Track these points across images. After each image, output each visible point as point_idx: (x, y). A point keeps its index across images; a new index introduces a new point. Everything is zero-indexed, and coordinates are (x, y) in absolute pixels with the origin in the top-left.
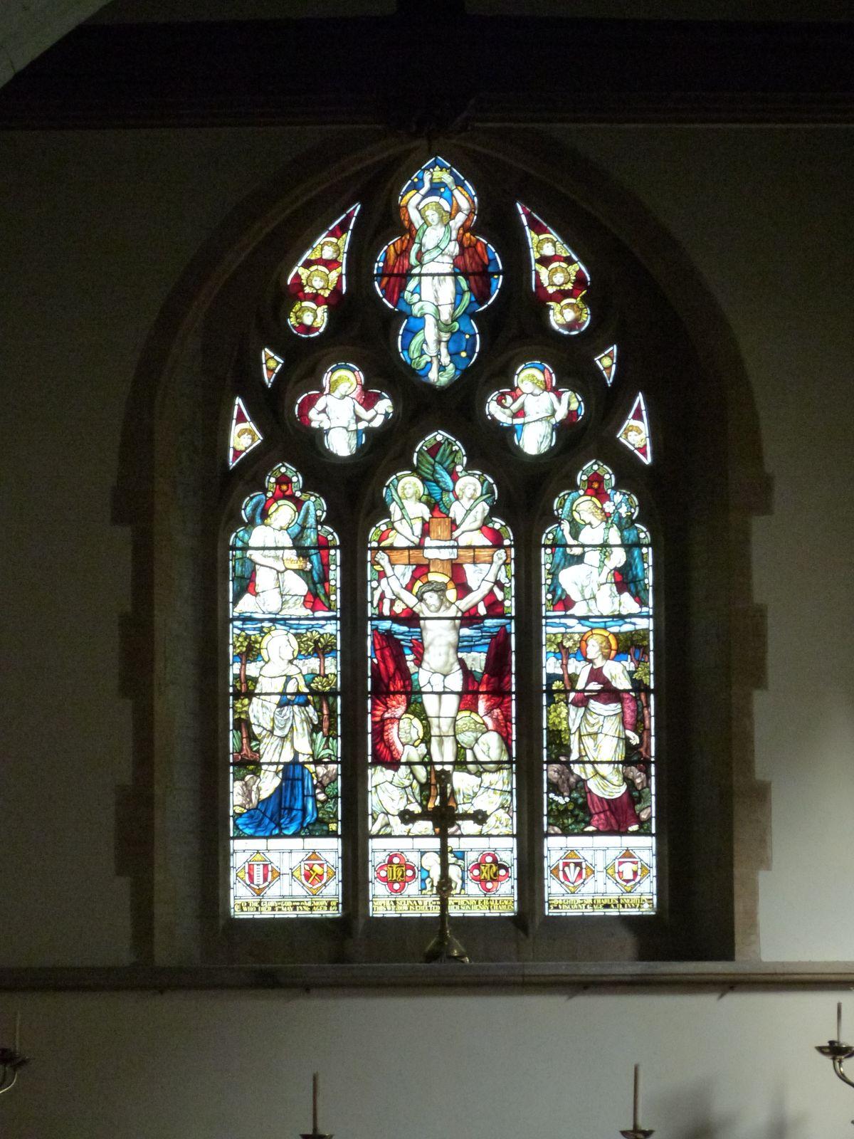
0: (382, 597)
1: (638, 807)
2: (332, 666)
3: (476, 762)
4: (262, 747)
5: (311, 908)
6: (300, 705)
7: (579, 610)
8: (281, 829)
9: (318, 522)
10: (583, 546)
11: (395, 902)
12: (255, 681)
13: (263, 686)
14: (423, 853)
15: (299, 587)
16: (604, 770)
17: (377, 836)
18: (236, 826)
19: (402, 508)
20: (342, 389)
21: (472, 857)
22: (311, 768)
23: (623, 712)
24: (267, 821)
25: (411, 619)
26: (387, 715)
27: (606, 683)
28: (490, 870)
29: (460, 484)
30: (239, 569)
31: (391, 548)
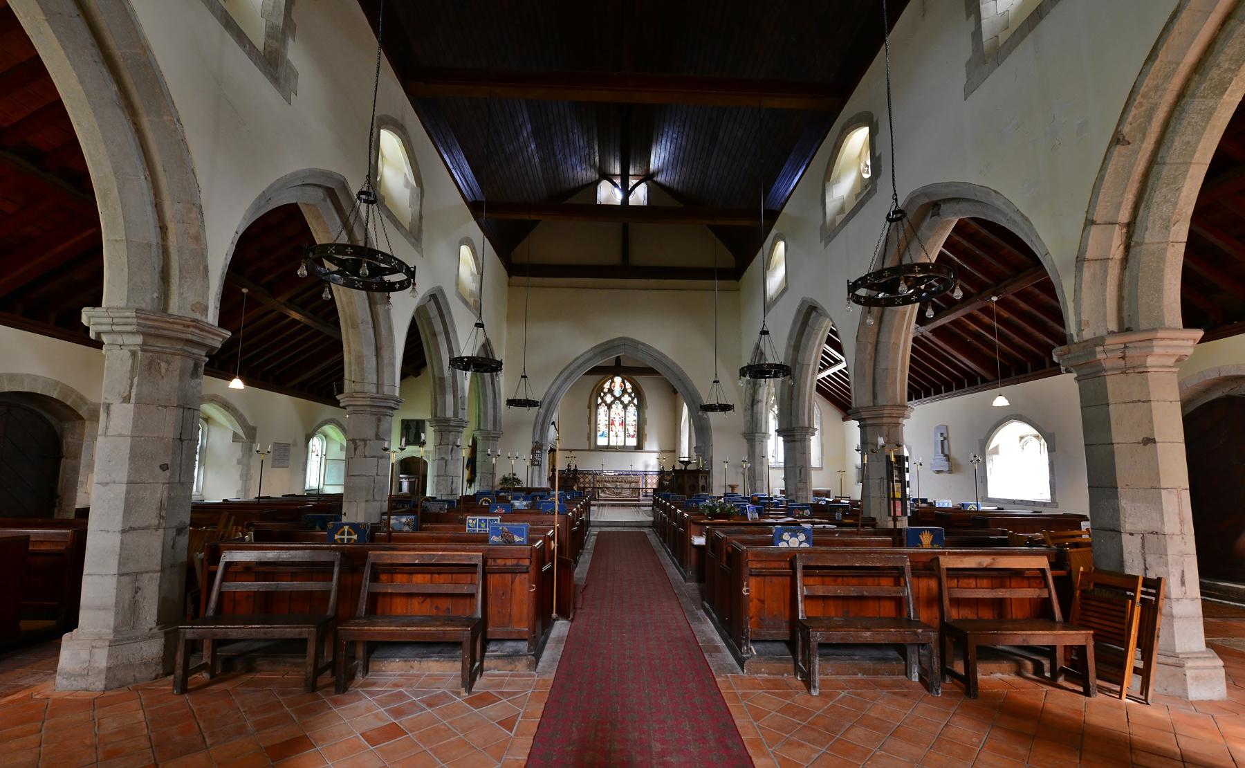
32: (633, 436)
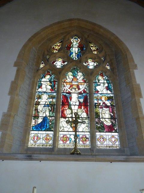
0: (64, 89)
1: (114, 127)
2: (54, 100)
3: (81, 118)
4: (40, 114)
5: (46, 146)
6: (48, 107)
7: (100, 92)
8: (41, 129)
9: (54, 78)
10: (100, 83)
11: (64, 145)
12: (40, 102)
13: (41, 103)
14: (70, 135)
15: (50, 88)
16: (107, 120)
17: (61, 131)
18: (32, 129)
19: (69, 77)
20: (60, 61)
21: (81, 136)
22: (49, 118)
23: (109, 110)
24: (39, 128)
25: (70, 93)
26: (64, 109)
27: (106, 105)
28: (85, 138)
29: (78, 74)
30: (39, 84)
31: (67, 82)
32: (111, 129)
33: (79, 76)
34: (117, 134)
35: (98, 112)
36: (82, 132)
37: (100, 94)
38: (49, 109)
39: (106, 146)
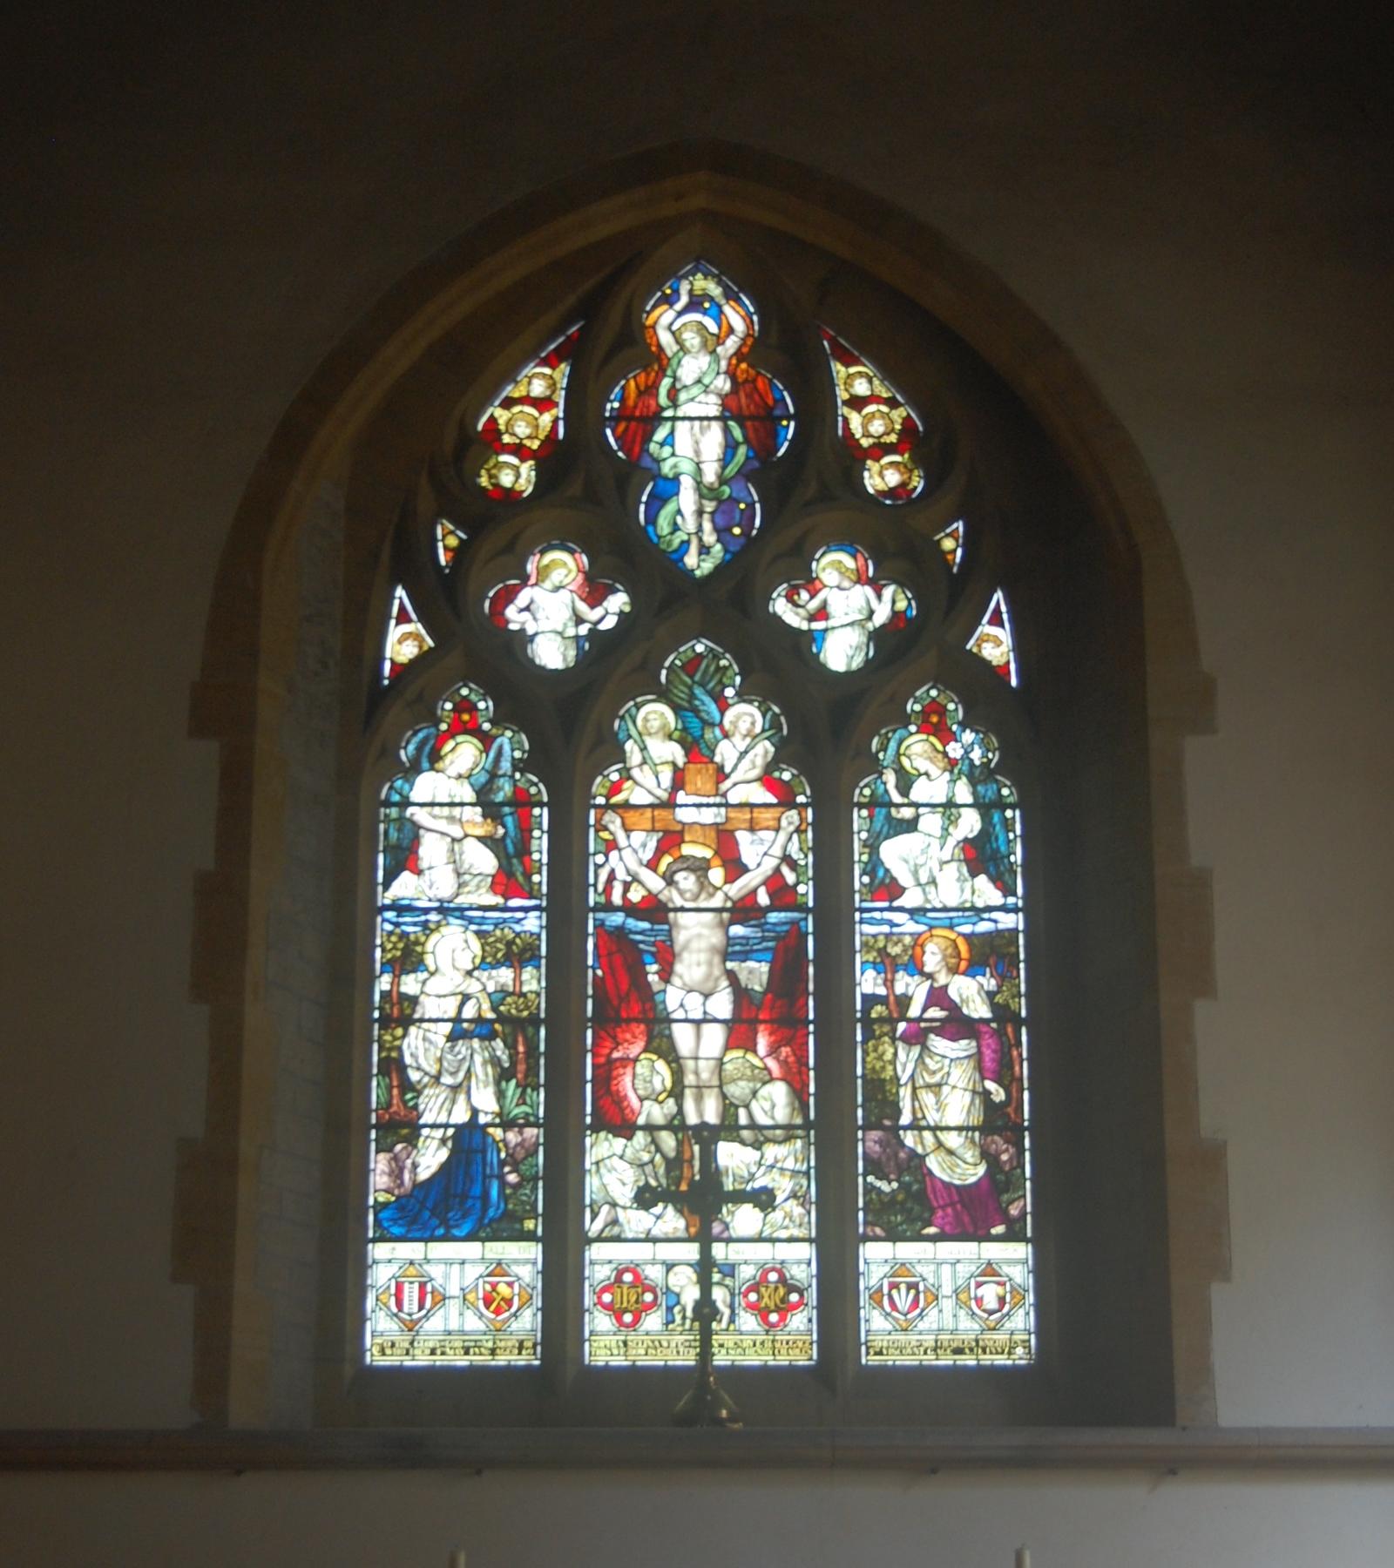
0: (612, 877)
1: (1005, 1197)
2: (532, 981)
3: (753, 1126)
5: (493, 1352)
6: (482, 1038)
7: (911, 899)
8: (448, 1228)
9: (515, 768)
10: (917, 805)
11: (625, 1343)
12: (414, 1001)
13: (429, 1008)
14: (669, 1267)
15: (484, 861)
17: (599, 1239)
19: (644, 749)
20: (557, 576)
21: (746, 1273)
22: (497, 1133)
24: (427, 1214)
25: (654, 909)
26: (616, 1055)
27: (953, 1008)
29: (730, 715)
30: (394, 835)
31: (626, 806)
33: (737, 739)
34: (1022, 1250)
35: (889, 1073)
36: (760, 1239)
37: (913, 912)
38: (495, 1061)
39: (929, 1340)
